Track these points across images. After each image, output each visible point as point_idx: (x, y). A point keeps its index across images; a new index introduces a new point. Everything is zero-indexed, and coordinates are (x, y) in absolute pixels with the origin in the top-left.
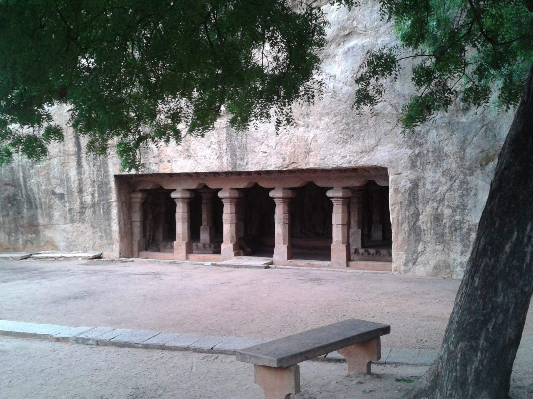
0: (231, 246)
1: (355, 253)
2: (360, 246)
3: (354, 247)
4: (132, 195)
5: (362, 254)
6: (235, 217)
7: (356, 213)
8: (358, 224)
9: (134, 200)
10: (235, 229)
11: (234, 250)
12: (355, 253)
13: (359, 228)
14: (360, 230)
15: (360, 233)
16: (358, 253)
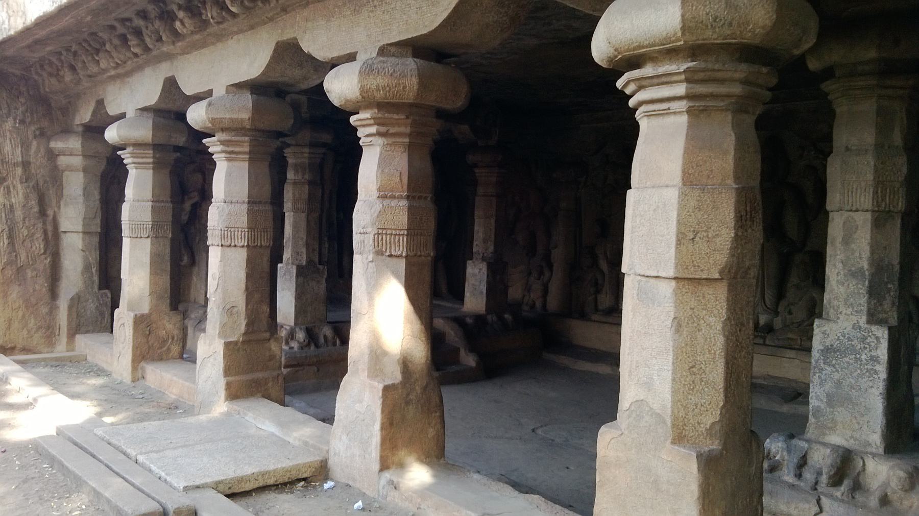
0: (218, 347)
1: (837, 480)
2: (875, 437)
3: (836, 439)
4: (53, 144)
5: (885, 501)
6: (243, 220)
7: (863, 220)
8: (875, 292)
9: (63, 161)
10: (242, 275)
11: (227, 372)
12: (837, 480)
13: (873, 318)
14: (882, 333)
15: (882, 352)
16: (857, 487)
